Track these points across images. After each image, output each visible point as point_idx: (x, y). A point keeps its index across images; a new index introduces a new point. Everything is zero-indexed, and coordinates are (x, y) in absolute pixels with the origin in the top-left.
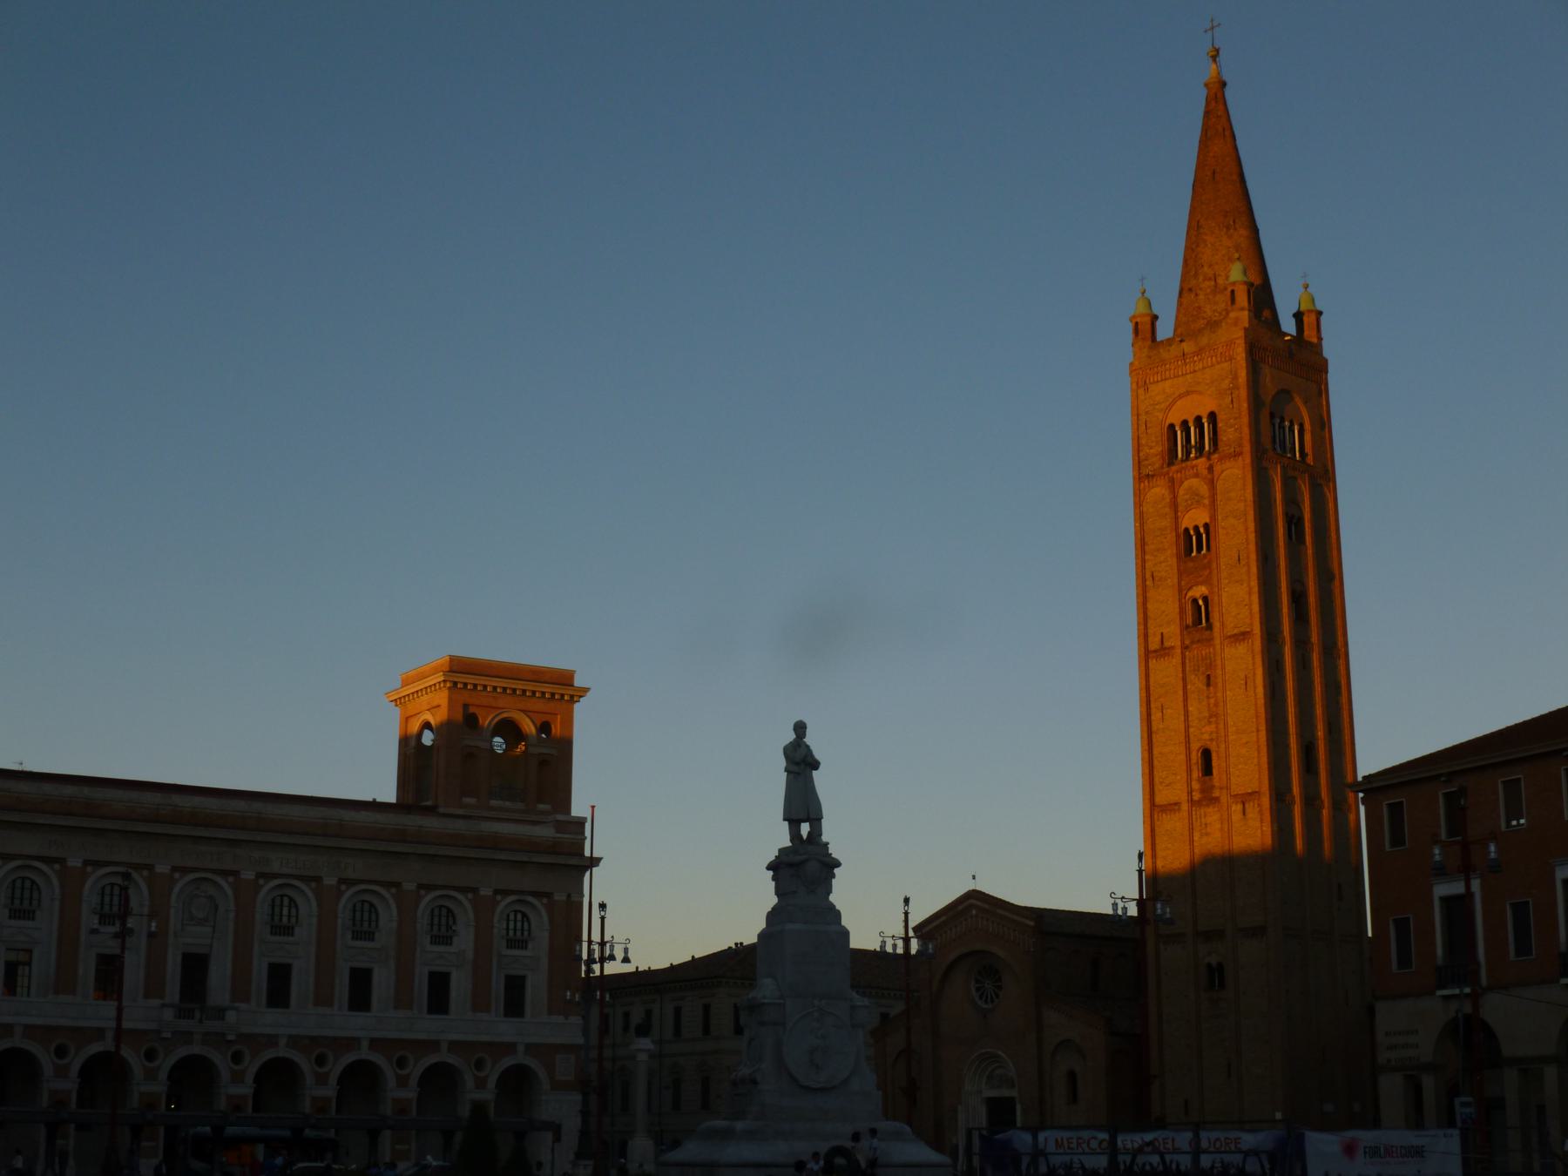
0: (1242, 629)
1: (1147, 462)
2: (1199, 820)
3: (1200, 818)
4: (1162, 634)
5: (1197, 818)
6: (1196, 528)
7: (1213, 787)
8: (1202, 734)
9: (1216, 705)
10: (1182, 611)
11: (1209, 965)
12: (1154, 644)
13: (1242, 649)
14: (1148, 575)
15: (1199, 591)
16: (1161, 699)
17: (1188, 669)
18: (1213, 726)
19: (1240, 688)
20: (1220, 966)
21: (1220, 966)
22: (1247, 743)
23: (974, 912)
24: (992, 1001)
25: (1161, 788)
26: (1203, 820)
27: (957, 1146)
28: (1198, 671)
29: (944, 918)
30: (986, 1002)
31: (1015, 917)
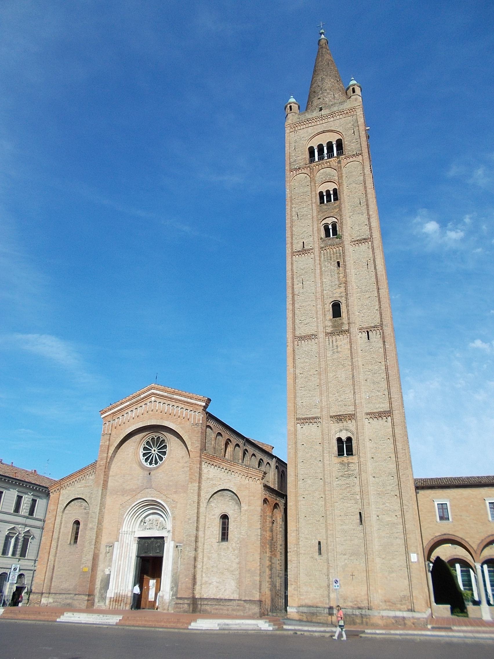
0: (365, 237)
1: (294, 163)
2: (331, 343)
3: (333, 343)
4: (303, 242)
5: (329, 343)
6: (328, 192)
7: (342, 323)
8: (333, 294)
9: (345, 276)
10: (319, 230)
11: (339, 440)
12: (299, 247)
13: (364, 247)
14: (294, 213)
15: (329, 221)
16: (303, 276)
17: (322, 259)
18: (343, 289)
19: (363, 267)
20: (349, 439)
21: (349, 439)
22: (369, 297)
23: (153, 399)
24: (156, 463)
25: (300, 326)
26: (334, 343)
27: (109, 575)
28: (331, 260)
29: (128, 403)
30: (151, 463)
31: (189, 400)
